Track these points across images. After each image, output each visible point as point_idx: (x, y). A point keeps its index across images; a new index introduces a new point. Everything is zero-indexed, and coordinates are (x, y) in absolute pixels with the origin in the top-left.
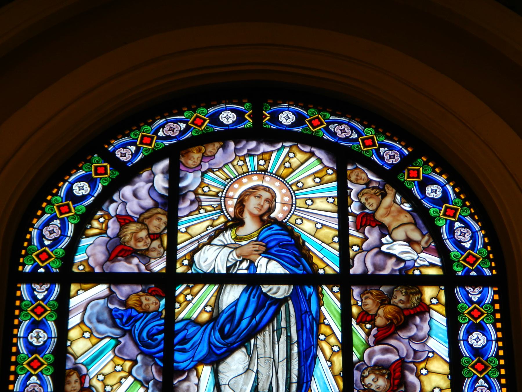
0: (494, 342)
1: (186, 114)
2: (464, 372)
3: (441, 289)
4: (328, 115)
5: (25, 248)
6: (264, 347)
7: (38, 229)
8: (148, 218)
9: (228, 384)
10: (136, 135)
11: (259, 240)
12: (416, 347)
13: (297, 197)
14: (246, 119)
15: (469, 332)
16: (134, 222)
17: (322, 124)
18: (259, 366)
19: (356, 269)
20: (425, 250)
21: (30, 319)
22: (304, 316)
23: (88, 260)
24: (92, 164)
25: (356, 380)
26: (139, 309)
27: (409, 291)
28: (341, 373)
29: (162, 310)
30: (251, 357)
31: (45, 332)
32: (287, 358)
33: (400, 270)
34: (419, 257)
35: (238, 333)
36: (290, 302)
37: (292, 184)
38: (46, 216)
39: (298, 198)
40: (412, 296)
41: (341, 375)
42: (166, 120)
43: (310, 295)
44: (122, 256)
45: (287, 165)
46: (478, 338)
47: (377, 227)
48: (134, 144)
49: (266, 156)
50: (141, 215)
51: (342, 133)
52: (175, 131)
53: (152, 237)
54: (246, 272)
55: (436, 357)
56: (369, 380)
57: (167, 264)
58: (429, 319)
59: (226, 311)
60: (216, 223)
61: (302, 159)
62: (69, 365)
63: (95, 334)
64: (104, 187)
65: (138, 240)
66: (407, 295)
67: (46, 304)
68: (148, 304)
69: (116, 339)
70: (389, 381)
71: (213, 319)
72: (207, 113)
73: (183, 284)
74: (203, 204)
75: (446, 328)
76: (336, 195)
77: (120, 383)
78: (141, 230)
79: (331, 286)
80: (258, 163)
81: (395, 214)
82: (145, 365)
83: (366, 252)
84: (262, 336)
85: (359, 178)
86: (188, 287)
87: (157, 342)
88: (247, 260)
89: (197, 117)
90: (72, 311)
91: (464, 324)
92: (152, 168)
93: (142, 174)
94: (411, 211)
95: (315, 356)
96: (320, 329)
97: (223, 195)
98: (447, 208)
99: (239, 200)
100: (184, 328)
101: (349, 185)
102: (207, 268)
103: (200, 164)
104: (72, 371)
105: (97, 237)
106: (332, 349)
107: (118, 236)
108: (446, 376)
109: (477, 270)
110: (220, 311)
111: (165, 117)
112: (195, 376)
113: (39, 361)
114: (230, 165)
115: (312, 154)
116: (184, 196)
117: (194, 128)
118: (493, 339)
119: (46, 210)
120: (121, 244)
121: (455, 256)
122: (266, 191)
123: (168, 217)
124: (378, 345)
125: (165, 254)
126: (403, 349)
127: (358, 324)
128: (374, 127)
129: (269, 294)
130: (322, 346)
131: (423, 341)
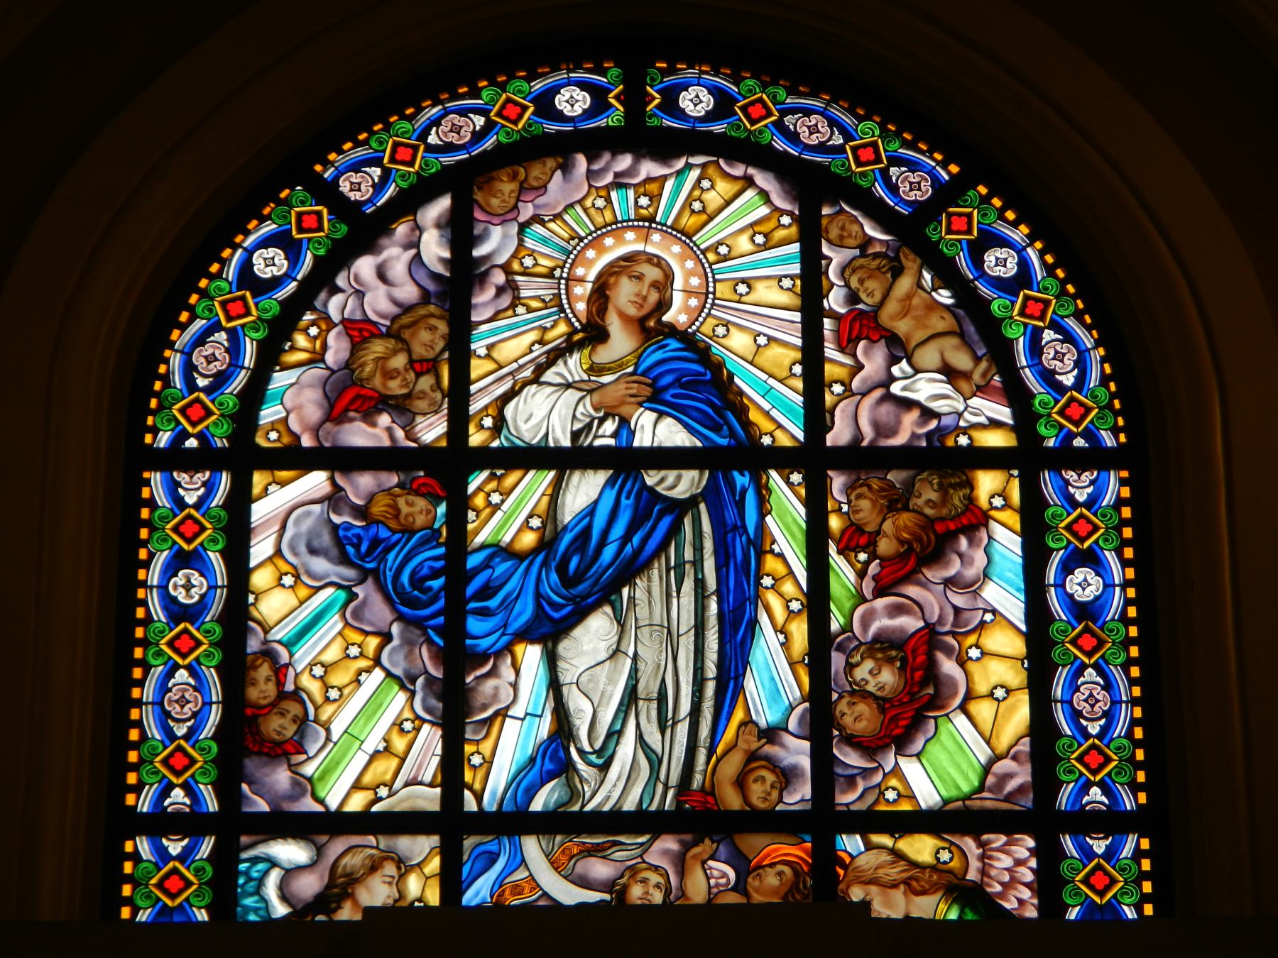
0: (1118, 590)
1: (485, 94)
2: (1056, 653)
3: (1012, 475)
4: (782, 94)
5: (157, 395)
6: (650, 602)
7: (182, 352)
8: (409, 326)
9: (577, 683)
10: (381, 143)
11: (640, 371)
12: (959, 601)
13: (717, 277)
14: (611, 106)
15: (1067, 569)
16: (381, 335)
17: (770, 114)
18: (638, 643)
19: (838, 435)
20: (983, 390)
21: (171, 548)
22: (730, 535)
23: (286, 418)
24: (292, 207)
25: (836, 673)
26: (393, 525)
27: (946, 482)
28: (806, 657)
29: (441, 526)
30: (622, 625)
31: (202, 575)
32: (696, 626)
33: (929, 435)
34: (967, 406)
35: (596, 575)
36: (702, 507)
37: (707, 249)
38: (199, 324)
39: (720, 281)
40: (951, 491)
41: (806, 662)
42: (445, 108)
43: (744, 491)
44: (356, 411)
45: (697, 206)
46: (1085, 580)
47: (883, 341)
48: (377, 162)
49: (653, 187)
50: (394, 319)
51: (811, 133)
52: (462, 132)
53: (417, 366)
54: (612, 442)
55: (999, 622)
56: (861, 673)
57: (449, 426)
58: (986, 540)
59: (570, 526)
60: (549, 336)
61: (727, 193)
62: (253, 645)
63: (305, 578)
64: (316, 257)
65: (389, 375)
66: (943, 489)
67: (203, 516)
68: (411, 514)
69: (348, 589)
71: (546, 545)
72: (530, 93)
73: (482, 469)
74: (524, 293)
75: (1020, 560)
76: (798, 271)
77: (358, 682)
78: (395, 352)
79: (787, 471)
80: (636, 202)
81: (920, 313)
82: (408, 643)
83: (859, 397)
84: (645, 580)
85: (845, 234)
86: (493, 476)
87: (430, 594)
88: (614, 416)
89: (509, 100)
90: (257, 531)
91: (1059, 550)
92: (415, 215)
93: (395, 229)
94: (953, 305)
95: (754, 622)
96: (764, 565)
97: (565, 275)
98: (1027, 298)
99: (596, 286)
100: (486, 565)
101: (826, 250)
102: (532, 434)
103: (516, 207)
104: (258, 658)
105: (305, 368)
106: (788, 607)
107: (347, 365)
108: (1020, 663)
109: (1089, 434)
110: (559, 529)
111: (441, 102)
113: (192, 637)
114: (578, 208)
115: (749, 182)
116: (483, 278)
117: (503, 126)
118: (1117, 582)
119: (199, 310)
120: (354, 384)
121: (1043, 404)
122: (653, 265)
123: (450, 325)
124: (881, 596)
125: (446, 406)
126: (932, 606)
127: (840, 552)
128: (878, 119)
129: (659, 489)
130: (767, 600)
131: (972, 587)
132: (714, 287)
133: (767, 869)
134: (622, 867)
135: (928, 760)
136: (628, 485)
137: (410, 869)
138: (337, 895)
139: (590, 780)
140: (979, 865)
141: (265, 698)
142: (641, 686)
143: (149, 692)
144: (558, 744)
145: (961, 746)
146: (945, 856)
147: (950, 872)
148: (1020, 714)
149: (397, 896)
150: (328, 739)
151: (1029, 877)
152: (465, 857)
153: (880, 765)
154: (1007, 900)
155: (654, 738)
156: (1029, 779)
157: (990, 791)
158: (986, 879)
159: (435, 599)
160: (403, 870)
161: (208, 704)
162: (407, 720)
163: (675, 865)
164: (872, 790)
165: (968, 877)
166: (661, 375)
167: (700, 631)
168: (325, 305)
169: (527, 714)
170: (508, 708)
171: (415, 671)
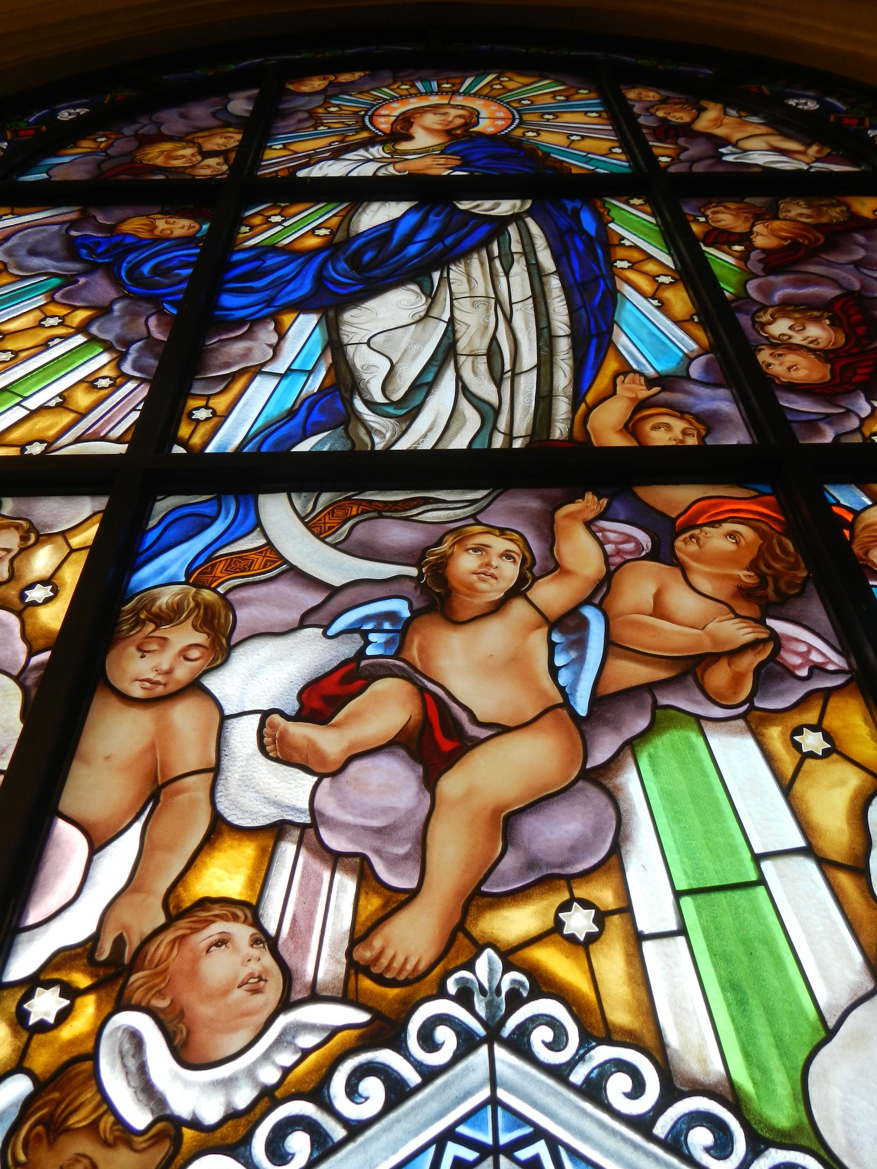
6: (469, 282)
28: (695, 317)
40: (825, 209)
49: (457, 81)
50: (187, 134)
59: (366, 234)
77: (45, 346)
82: (131, 315)
107: (130, 153)
112: (272, 331)
126: (849, 279)
127: (707, 245)
130: (625, 276)
133: (706, 529)
136: (437, 210)
137: (43, 538)
139: (383, 430)
152: (152, 523)
155: (485, 389)
159: (181, 282)
162: (104, 378)
163: (537, 528)
167: (540, 299)
169: (290, 371)
170: (263, 365)
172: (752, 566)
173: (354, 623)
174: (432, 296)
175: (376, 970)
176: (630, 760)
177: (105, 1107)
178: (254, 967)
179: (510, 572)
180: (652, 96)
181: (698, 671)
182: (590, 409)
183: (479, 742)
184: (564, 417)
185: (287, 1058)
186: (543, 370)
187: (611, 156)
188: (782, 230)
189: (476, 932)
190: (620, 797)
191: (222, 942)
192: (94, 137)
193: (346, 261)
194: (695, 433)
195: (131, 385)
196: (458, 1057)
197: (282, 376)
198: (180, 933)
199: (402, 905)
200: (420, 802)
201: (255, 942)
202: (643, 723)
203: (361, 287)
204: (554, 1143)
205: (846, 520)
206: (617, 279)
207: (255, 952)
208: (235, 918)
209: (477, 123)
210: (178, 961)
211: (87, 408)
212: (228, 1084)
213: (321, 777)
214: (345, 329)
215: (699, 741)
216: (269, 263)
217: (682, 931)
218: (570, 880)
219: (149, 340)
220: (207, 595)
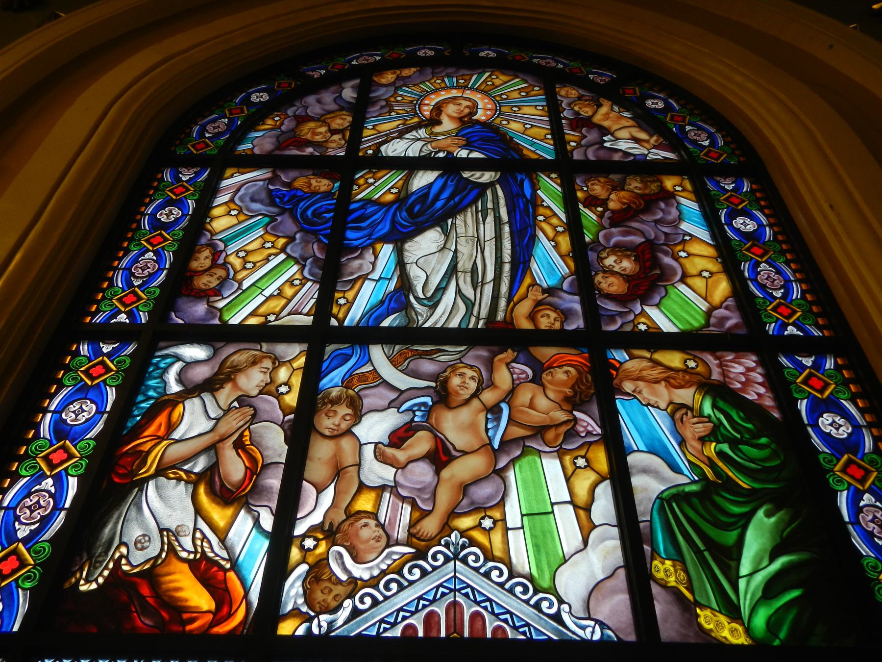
0: (767, 229)
3: (684, 178)
6: (465, 226)
18: (458, 245)
20: (655, 147)
26: (306, 190)
30: (447, 235)
32: (496, 237)
36: (498, 186)
40: (649, 184)
43: (522, 181)
44: (294, 146)
45: (489, 83)
46: (744, 222)
49: (467, 77)
50: (322, 116)
62: (203, 241)
65: (315, 134)
66: (642, 182)
70: (638, 264)
77: (267, 260)
78: (321, 126)
79: (548, 173)
80: (457, 81)
81: (614, 119)
82: (305, 242)
87: (324, 220)
89: (393, 53)
91: (723, 209)
104: (203, 247)
107: (293, 130)
108: (715, 260)
110: (409, 193)
115: (517, 77)
118: (765, 223)
124: (615, 227)
126: (649, 232)
127: (585, 207)
132: (500, 108)
133: (556, 369)
134: (446, 365)
135: (664, 308)
136: (452, 177)
137: (282, 364)
138: (220, 380)
139: (423, 313)
140: (719, 370)
141: (202, 267)
142: (460, 266)
143: (124, 263)
144: (401, 294)
145: (686, 301)
146: (691, 364)
147: (698, 374)
148: (722, 288)
149: (269, 380)
150: (239, 288)
151: (760, 379)
152: (326, 357)
153: (631, 311)
154: (749, 394)
155: (468, 291)
156: (740, 320)
157: (714, 326)
158: (727, 380)
159: (327, 222)
160: (277, 364)
161: (160, 270)
162: (297, 279)
163: (486, 366)
164: (628, 324)
165: (713, 378)
166: (472, 137)
167: (499, 239)
168: (286, 110)
169: (380, 278)
170: (368, 274)
171: (307, 255)
172: (572, 387)
173: (409, 407)
174: (446, 234)
175: (418, 536)
176: (512, 467)
177: (332, 574)
178: (377, 534)
179: (473, 386)
180: (574, 93)
181: (543, 433)
182: (515, 305)
183: (457, 458)
184: (503, 309)
185: (389, 562)
186: (496, 282)
187: (545, 141)
188: (625, 198)
189: (452, 525)
190: (506, 480)
191: (366, 525)
192: (272, 116)
193: (406, 211)
194: (560, 320)
195: (309, 284)
196: (444, 563)
197: (377, 281)
198: (351, 522)
199: (427, 515)
200: (434, 479)
201: (377, 526)
202: (518, 453)
203: (413, 228)
204: (473, 589)
205: (616, 366)
206: (537, 227)
207: (377, 529)
208: (370, 518)
209: (476, 113)
210: (351, 531)
211: (291, 296)
212: (371, 568)
213: (398, 469)
214: (406, 254)
215: (538, 461)
216: (369, 211)
217: (522, 528)
218: (485, 509)
219: (316, 260)
220: (350, 392)
